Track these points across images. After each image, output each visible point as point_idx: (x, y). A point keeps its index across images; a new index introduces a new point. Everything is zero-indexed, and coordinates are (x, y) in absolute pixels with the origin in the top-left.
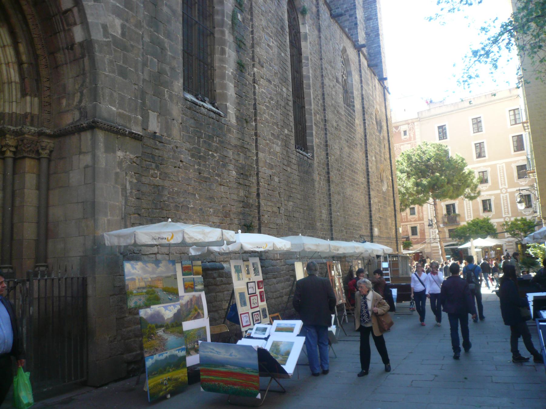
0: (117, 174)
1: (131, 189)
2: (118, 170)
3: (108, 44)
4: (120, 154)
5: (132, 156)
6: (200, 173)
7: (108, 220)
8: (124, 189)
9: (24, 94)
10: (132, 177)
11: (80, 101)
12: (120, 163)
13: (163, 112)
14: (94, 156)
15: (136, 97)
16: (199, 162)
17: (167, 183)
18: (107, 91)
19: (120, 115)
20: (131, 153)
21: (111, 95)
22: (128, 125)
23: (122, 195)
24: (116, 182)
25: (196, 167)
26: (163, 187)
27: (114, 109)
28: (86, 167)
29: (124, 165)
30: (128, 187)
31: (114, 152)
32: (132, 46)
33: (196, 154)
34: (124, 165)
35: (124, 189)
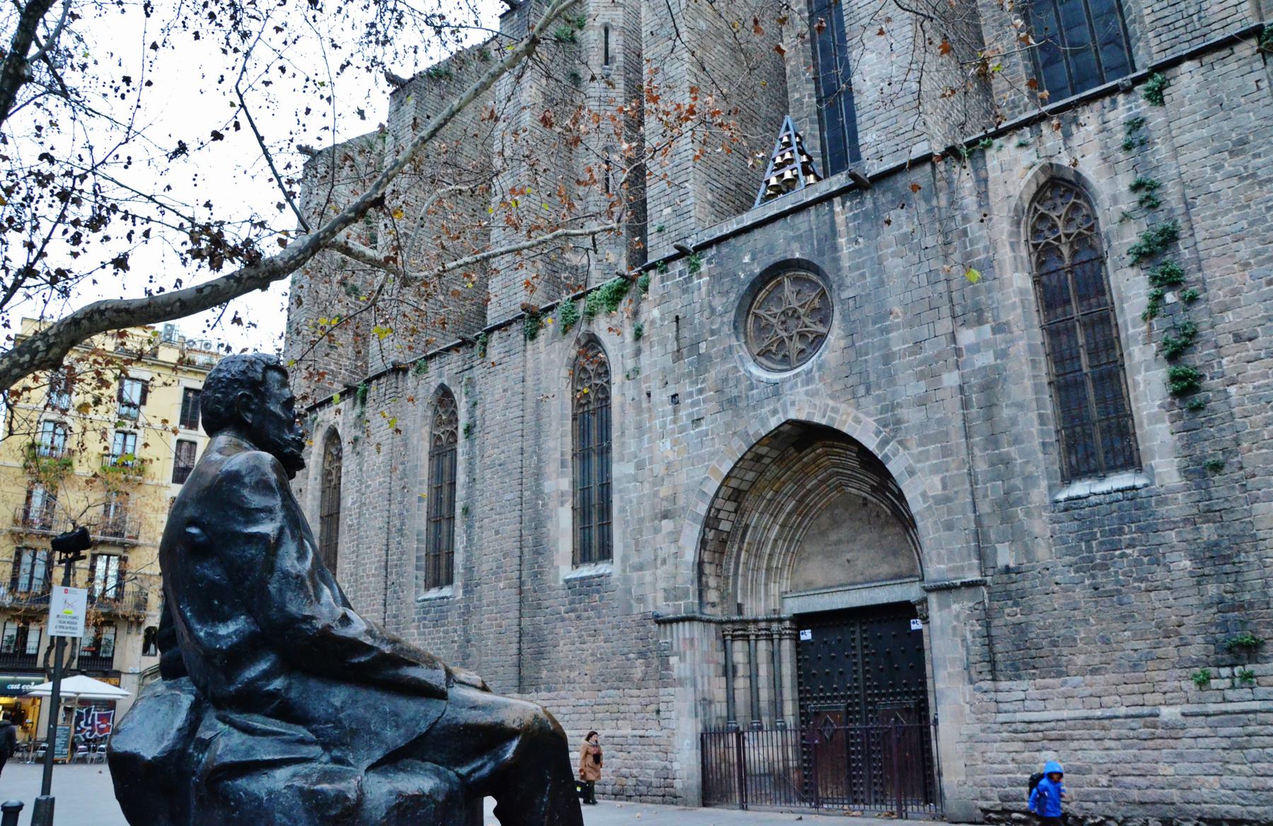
0: (954, 628)
1: (974, 637)
2: (955, 623)
3: (929, 507)
4: (956, 607)
5: (971, 604)
6: (1096, 589)
7: (949, 673)
8: (964, 640)
10: (972, 625)
12: (957, 617)
13: (1017, 536)
15: (968, 542)
16: (1091, 575)
17: (1034, 618)
18: (934, 553)
19: (951, 570)
20: (970, 601)
21: (939, 554)
22: (961, 575)
23: (963, 646)
24: (954, 635)
25: (1087, 582)
27: (942, 566)
29: (962, 617)
30: (969, 636)
31: (949, 606)
32: (956, 493)
33: (1086, 566)
34: (962, 617)
35: (964, 640)
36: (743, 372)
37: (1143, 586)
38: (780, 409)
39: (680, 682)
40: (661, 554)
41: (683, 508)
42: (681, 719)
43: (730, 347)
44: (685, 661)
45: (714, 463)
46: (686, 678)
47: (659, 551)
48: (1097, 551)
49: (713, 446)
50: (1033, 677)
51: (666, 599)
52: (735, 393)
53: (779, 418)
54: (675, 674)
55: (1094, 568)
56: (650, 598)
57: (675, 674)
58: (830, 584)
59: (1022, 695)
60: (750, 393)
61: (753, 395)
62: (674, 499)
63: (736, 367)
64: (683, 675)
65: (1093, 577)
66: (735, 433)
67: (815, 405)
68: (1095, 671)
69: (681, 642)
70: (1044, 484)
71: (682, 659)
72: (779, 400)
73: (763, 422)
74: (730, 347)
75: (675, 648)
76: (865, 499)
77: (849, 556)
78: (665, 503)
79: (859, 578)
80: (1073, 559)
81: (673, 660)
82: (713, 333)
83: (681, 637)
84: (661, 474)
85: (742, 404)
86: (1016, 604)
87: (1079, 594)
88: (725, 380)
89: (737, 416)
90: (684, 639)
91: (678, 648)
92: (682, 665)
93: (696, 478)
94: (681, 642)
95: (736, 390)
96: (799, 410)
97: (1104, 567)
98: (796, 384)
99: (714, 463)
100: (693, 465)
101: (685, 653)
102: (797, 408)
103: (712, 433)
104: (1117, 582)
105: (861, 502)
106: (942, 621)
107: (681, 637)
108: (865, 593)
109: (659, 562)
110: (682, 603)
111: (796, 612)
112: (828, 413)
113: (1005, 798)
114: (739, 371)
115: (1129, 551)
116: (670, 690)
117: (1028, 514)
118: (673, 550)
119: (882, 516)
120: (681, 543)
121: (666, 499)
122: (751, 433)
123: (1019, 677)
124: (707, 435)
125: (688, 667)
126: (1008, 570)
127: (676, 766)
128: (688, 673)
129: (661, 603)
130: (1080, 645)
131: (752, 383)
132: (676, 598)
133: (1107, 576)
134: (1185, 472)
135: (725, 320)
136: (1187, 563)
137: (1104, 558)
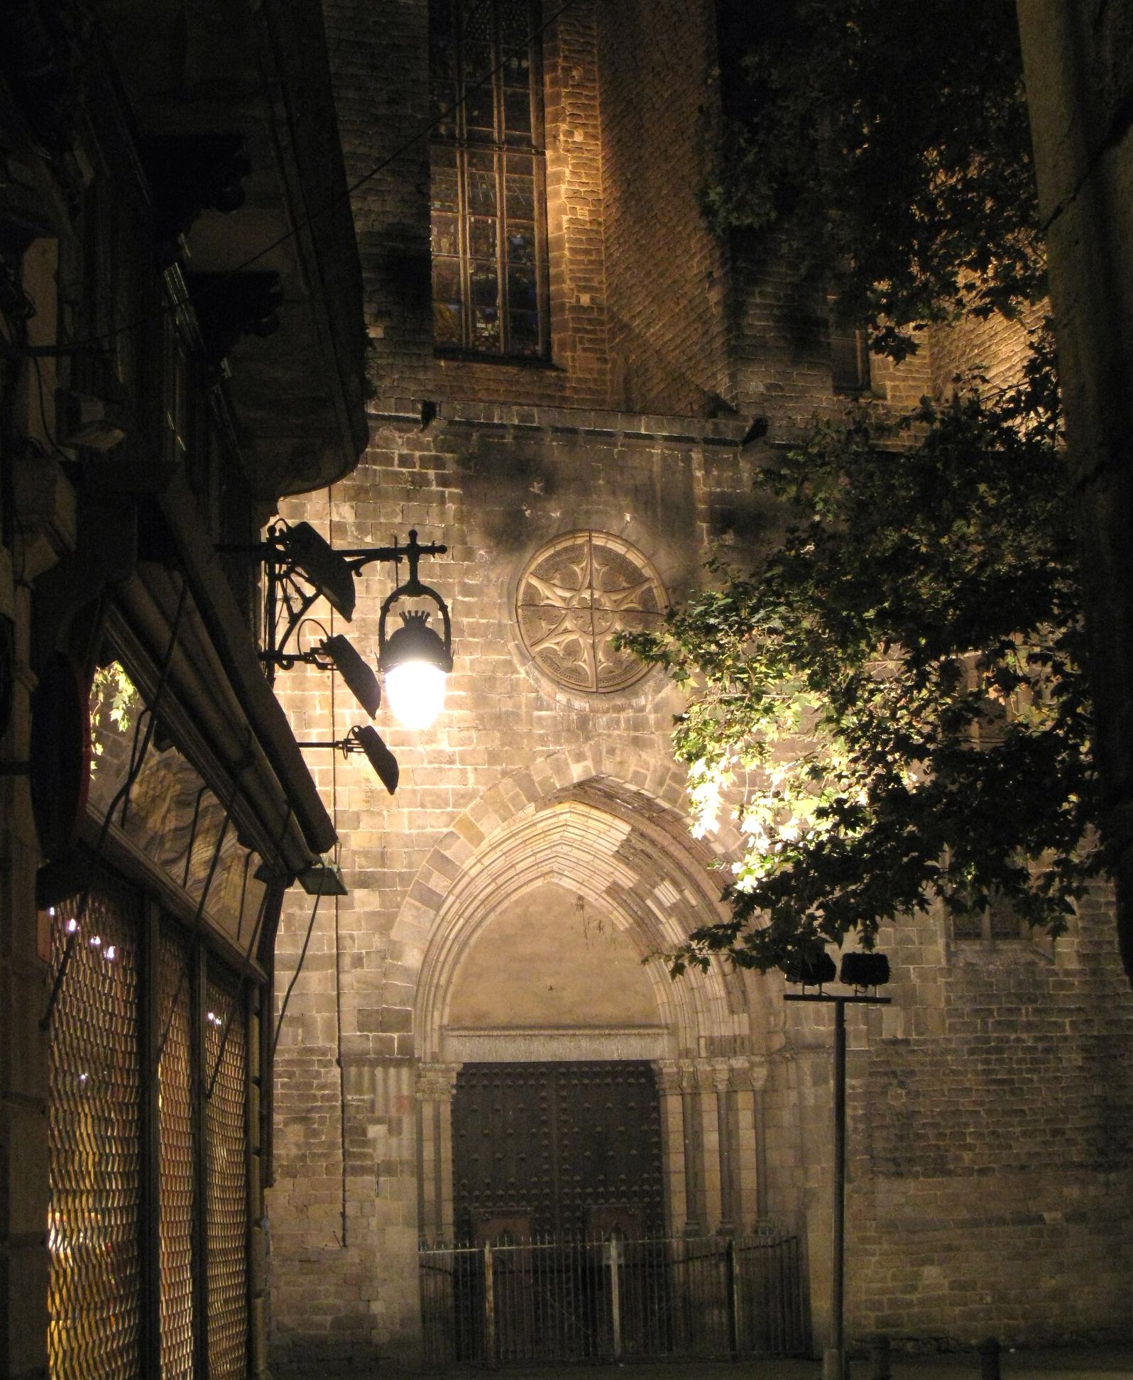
7: (823, 1169)
9: (732, 1012)
11: (785, 1023)
14: (801, 1097)
25: (980, 1067)
26: (914, 1113)
27: (822, 1028)
28: (794, 1105)
36: (523, 675)
37: (1035, 1077)
38: (588, 754)
39: (389, 1168)
40: (351, 950)
41: (400, 874)
42: (390, 1229)
43: (500, 624)
44: (400, 1133)
45: (466, 811)
46: (401, 1162)
47: (347, 942)
48: (995, 1031)
49: (464, 781)
50: (916, 1176)
51: (362, 1026)
52: (507, 706)
53: (586, 768)
54: (379, 1154)
55: (988, 1052)
56: (320, 1018)
57: (379, 1154)
58: (515, 1022)
59: (903, 1200)
60: (536, 713)
61: (540, 718)
62: (382, 858)
63: (509, 663)
64: (394, 1157)
65: (987, 1062)
66: (504, 774)
67: (647, 763)
68: (982, 1172)
69: (392, 1102)
70: (941, 942)
71: (394, 1128)
72: (587, 739)
73: (560, 769)
74: (500, 624)
75: (379, 1112)
76: (581, 898)
77: (550, 982)
78: (363, 861)
79: (567, 1020)
80: (969, 1036)
81: (374, 1131)
82: (467, 590)
83: (393, 1091)
84: (354, 809)
85: (522, 728)
86: (902, 1084)
87: (970, 1080)
88: (491, 680)
89: (510, 744)
90: (399, 1098)
91: (387, 1111)
92: (394, 1141)
93: (429, 830)
94: (392, 1102)
95: (510, 703)
96: (621, 763)
97: (999, 1050)
98: (618, 722)
99: (466, 811)
100: (423, 806)
101: (400, 1120)
102: (618, 759)
103: (463, 762)
104: (1010, 1071)
105: (574, 901)
106: (816, 1097)
107: (393, 1091)
108: (584, 1043)
109: (346, 961)
110: (395, 1035)
111: (467, 1060)
112: (668, 781)
113: (884, 1322)
114: (515, 671)
115: (1024, 1036)
116: (369, 1178)
117: (923, 976)
118: (377, 942)
119: (608, 929)
120: (394, 934)
121: (365, 854)
122: (537, 778)
123: (900, 1175)
124: (452, 762)
125: (405, 1143)
126: (895, 1042)
127: (377, 1307)
128: (406, 1155)
129: (350, 1032)
130: (969, 1140)
131: (539, 698)
132: (383, 1027)
133: (1000, 1061)
134: (1083, 957)
135: (493, 576)
136: (1077, 1059)
137: (999, 1039)
